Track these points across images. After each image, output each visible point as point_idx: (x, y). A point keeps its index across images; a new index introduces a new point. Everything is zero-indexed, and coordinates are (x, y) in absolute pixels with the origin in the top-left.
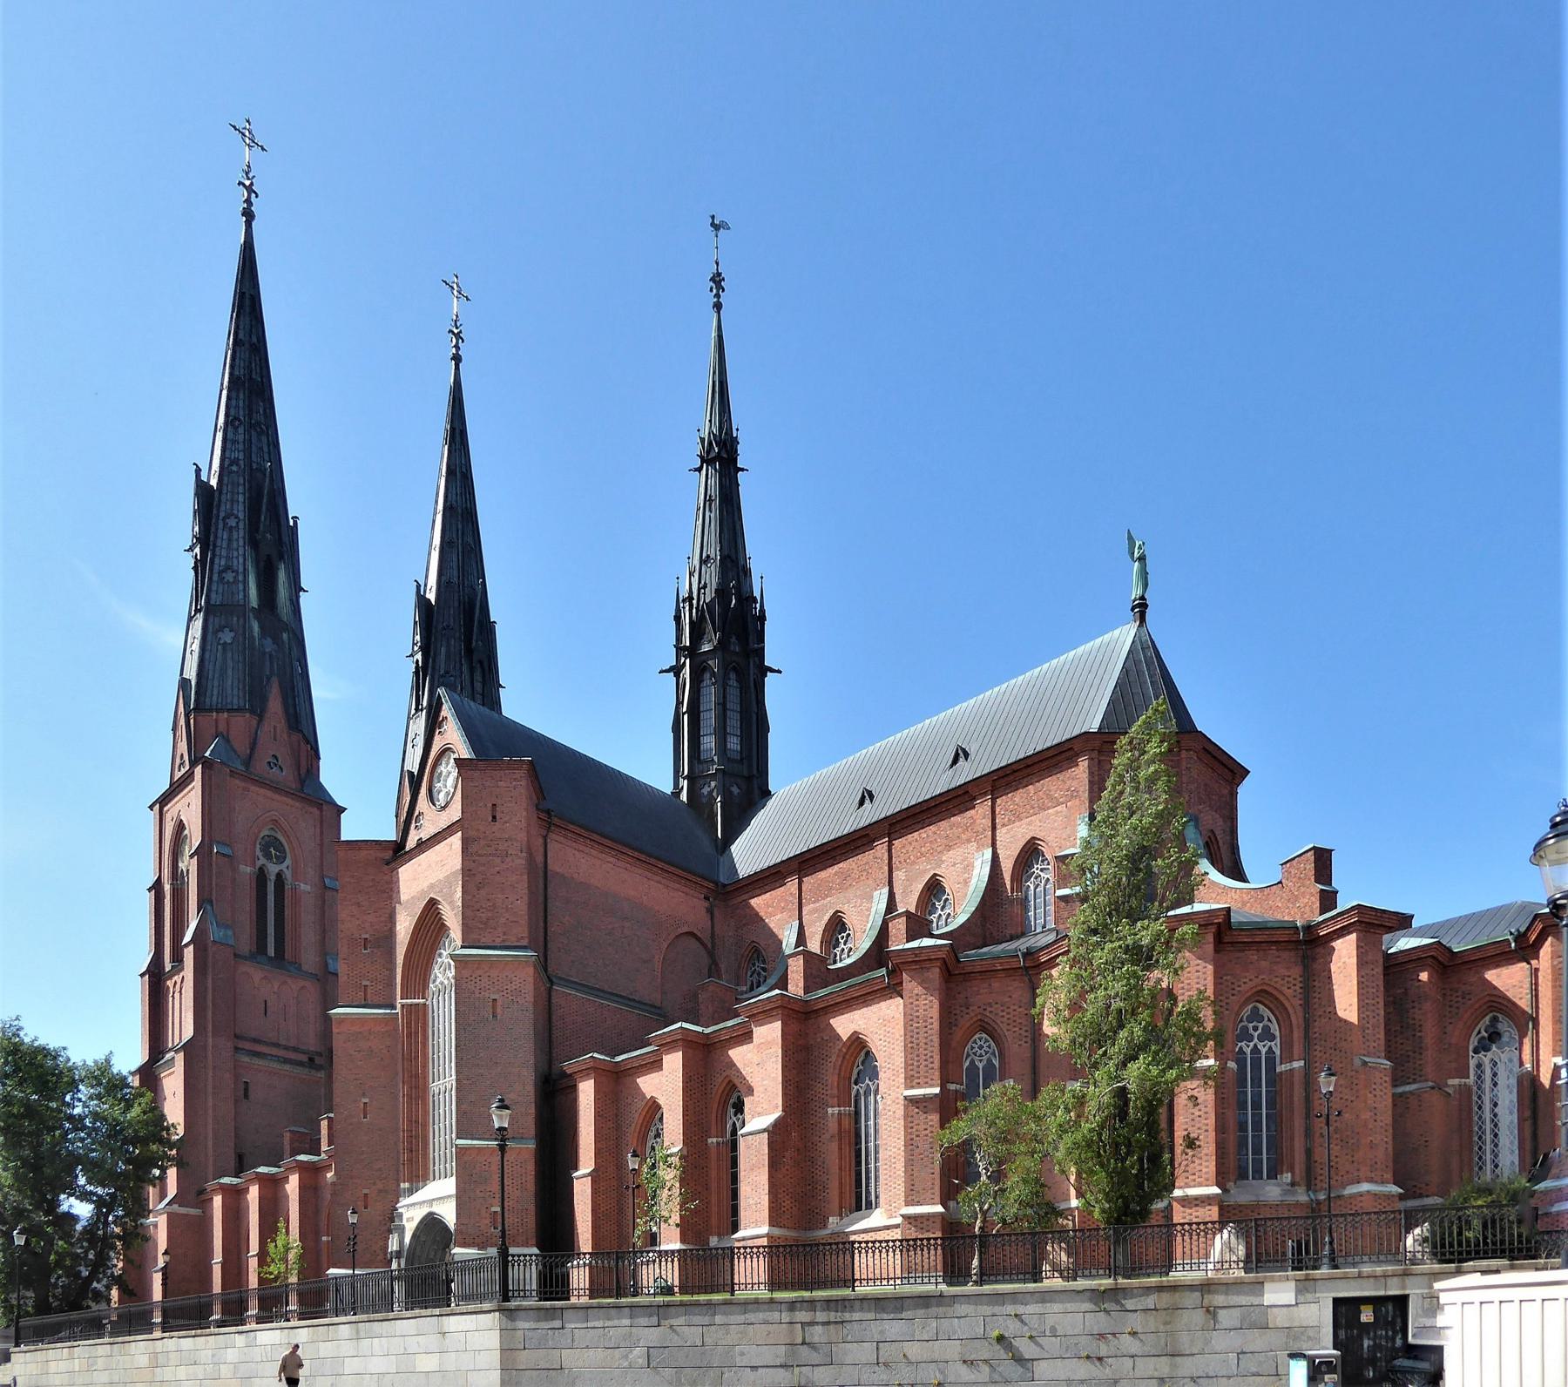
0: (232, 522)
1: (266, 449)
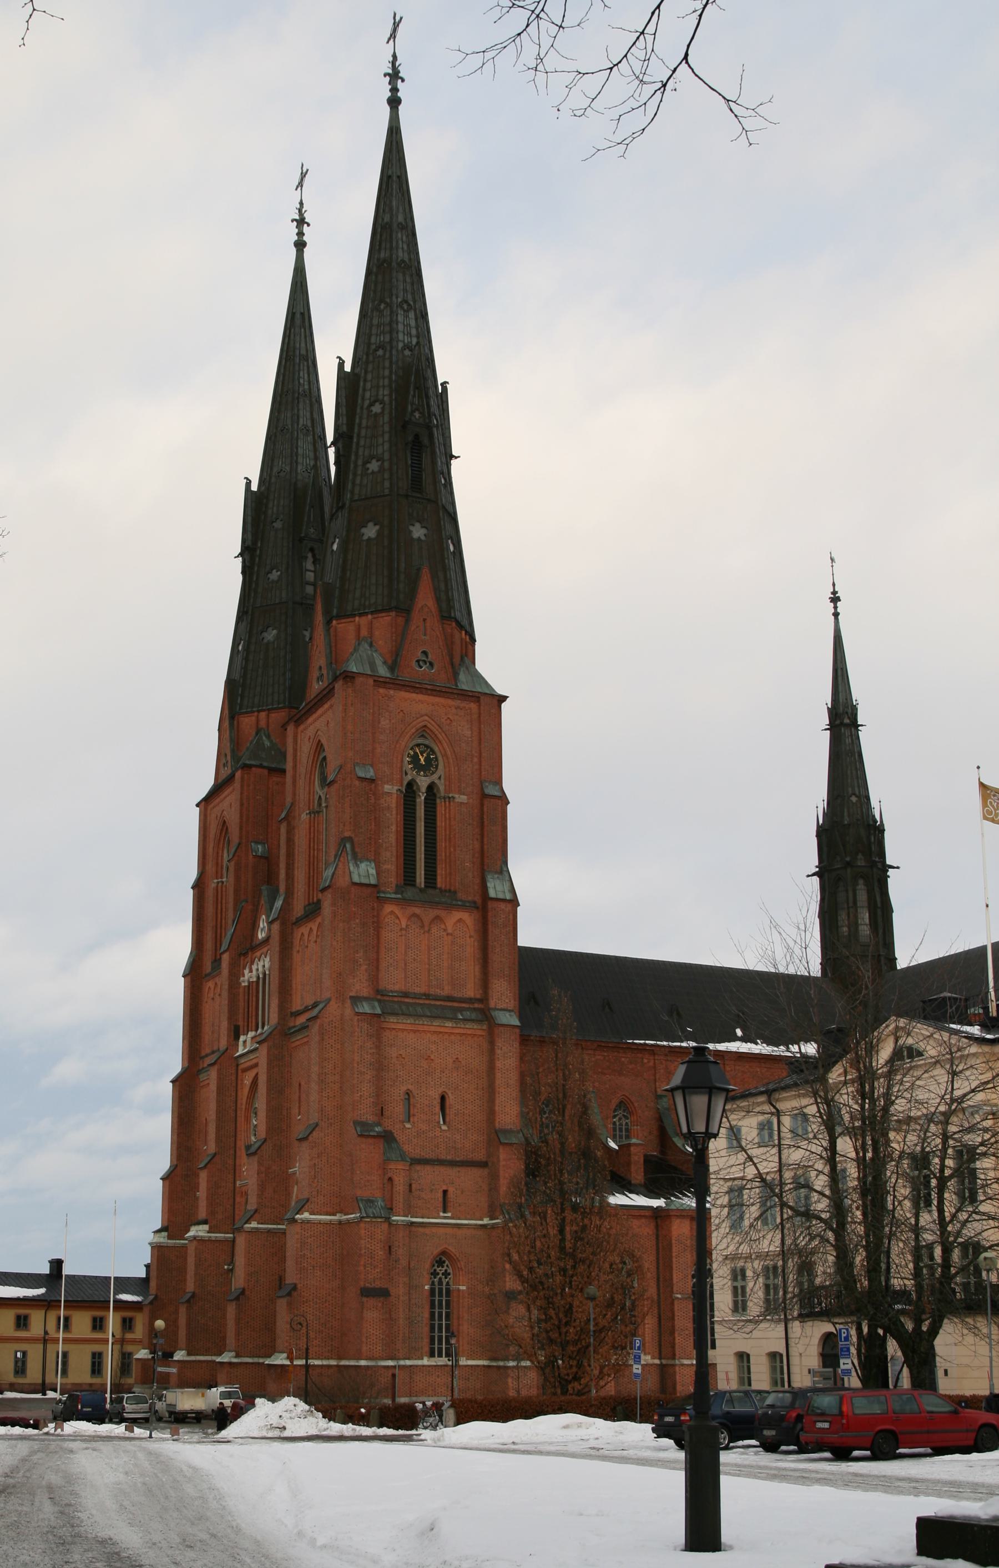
0: (377, 409)
1: (413, 323)
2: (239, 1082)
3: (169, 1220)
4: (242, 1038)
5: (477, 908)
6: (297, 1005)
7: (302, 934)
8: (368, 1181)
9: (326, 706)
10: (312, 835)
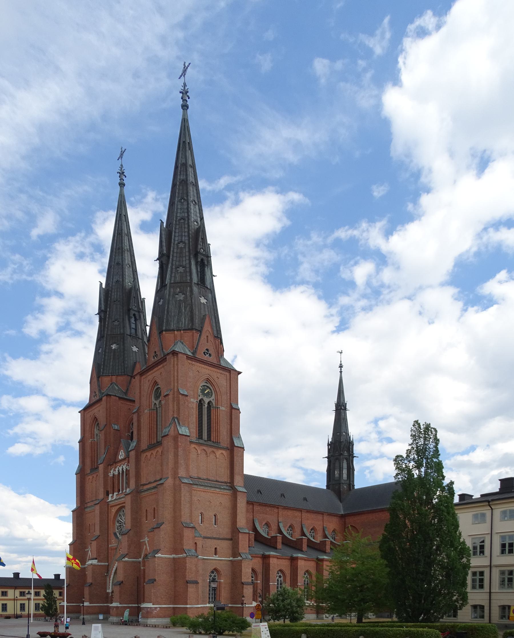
2: (109, 511)
4: (110, 495)
5: (229, 449)
7: (147, 455)
8: (188, 543)
9: (161, 366)
10: (151, 418)
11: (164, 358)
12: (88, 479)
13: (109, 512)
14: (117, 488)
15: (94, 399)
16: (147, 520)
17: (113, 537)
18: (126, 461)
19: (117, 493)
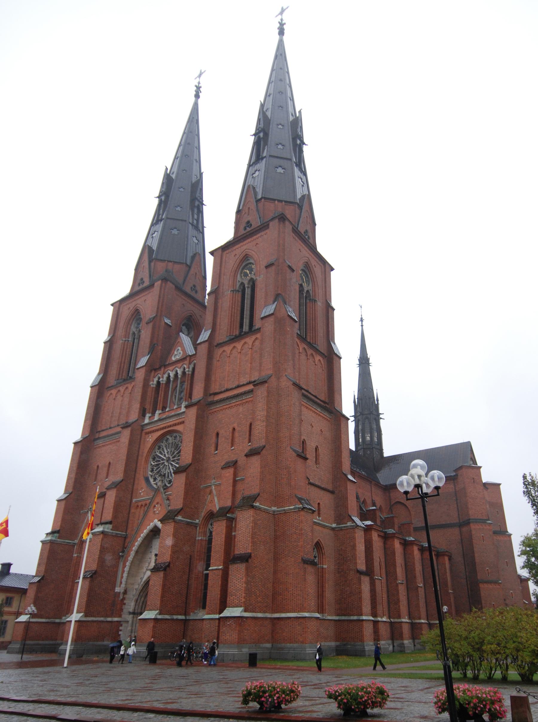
2: (142, 440)
3: (61, 526)
4: (148, 415)
6: (215, 388)
11: (266, 224)
12: (109, 394)
13: (142, 441)
14: (161, 403)
15: (137, 288)
16: (217, 450)
17: (143, 483)
18: (185, 362)
19: (160, 412)
